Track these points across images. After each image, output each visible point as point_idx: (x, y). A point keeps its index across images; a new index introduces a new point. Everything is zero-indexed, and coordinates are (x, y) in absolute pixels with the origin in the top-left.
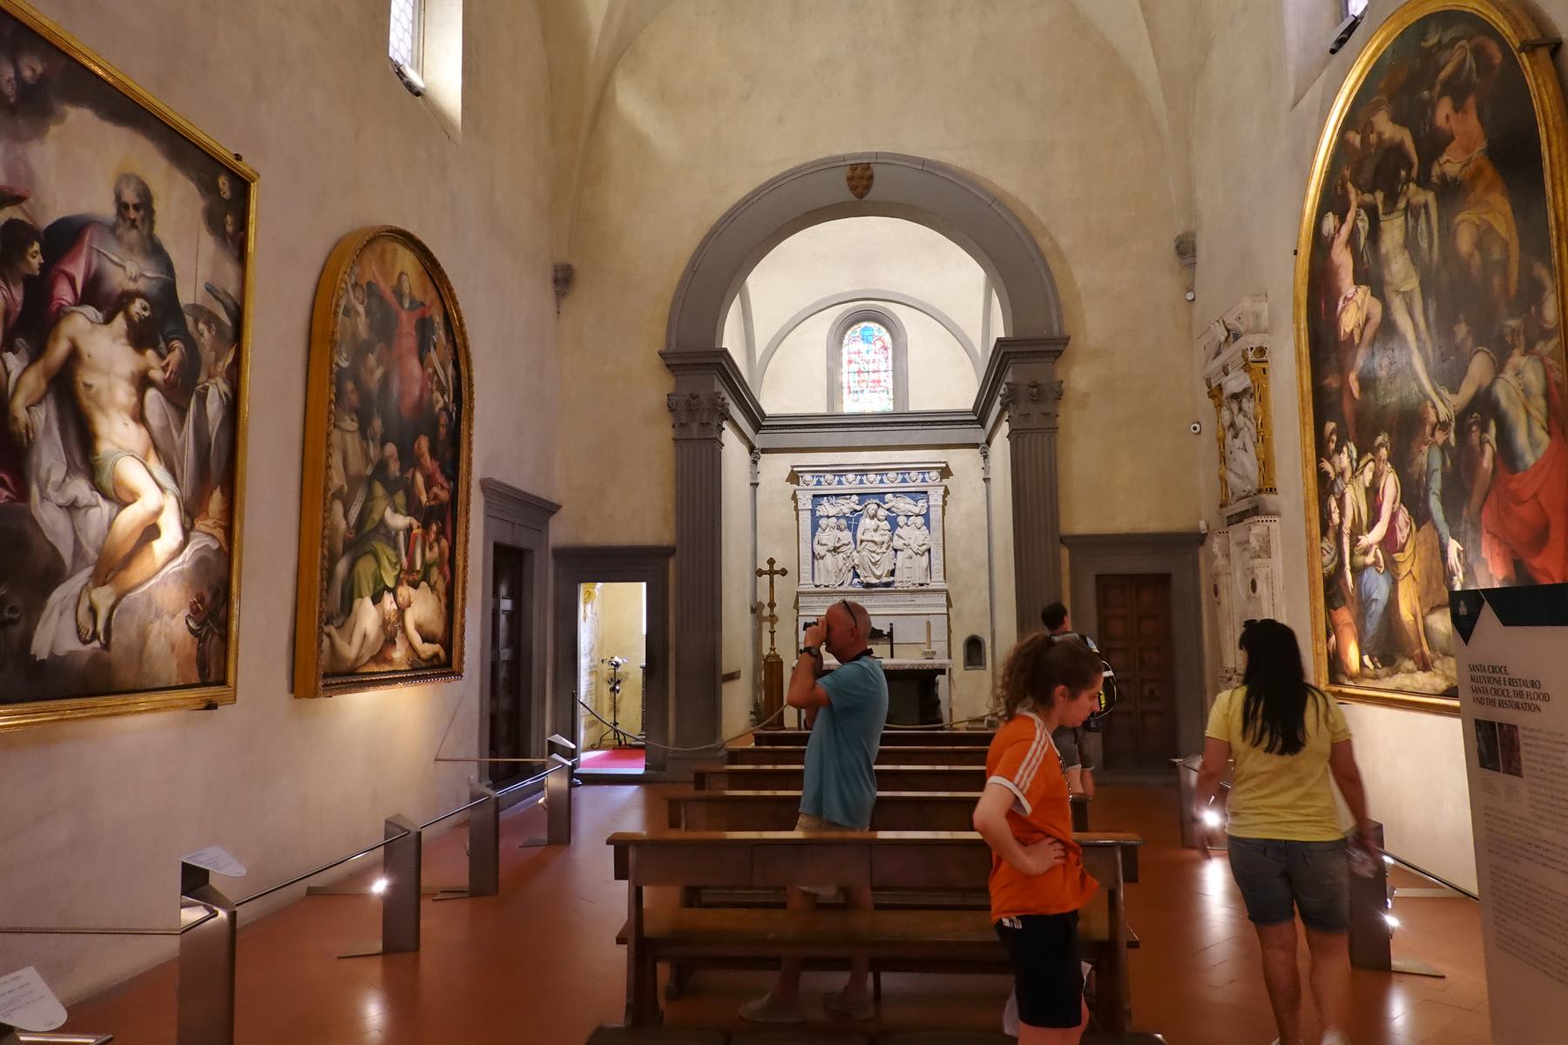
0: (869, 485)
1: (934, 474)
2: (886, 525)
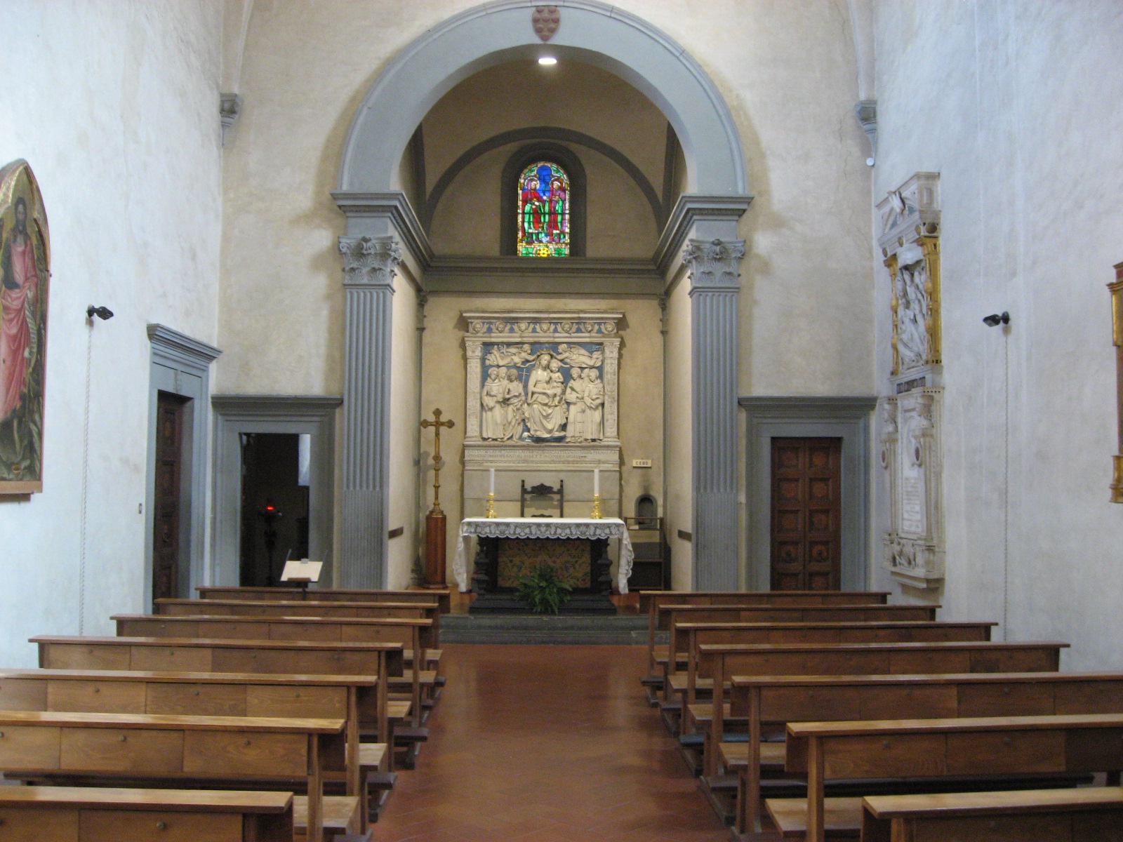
0: (542, 334)
1: (610, 327)
2: (558, 376)
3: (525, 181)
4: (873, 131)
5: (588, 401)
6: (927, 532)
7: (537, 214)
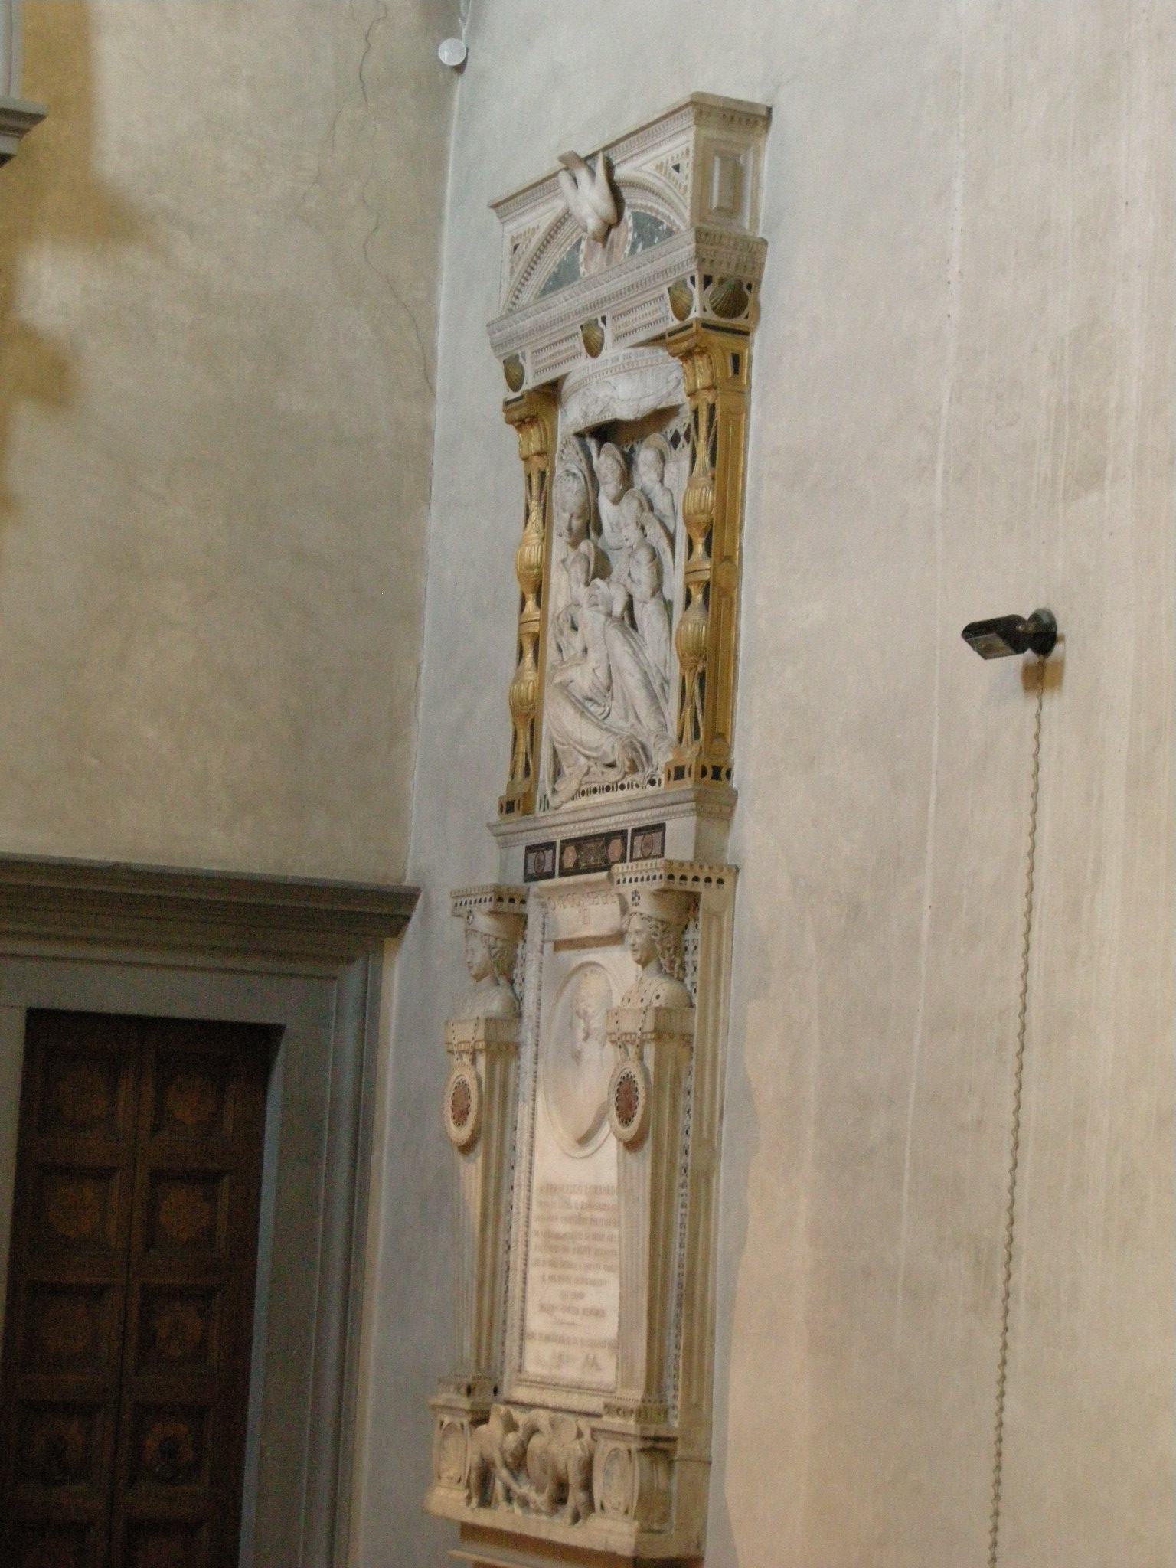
6: (648, 1390)
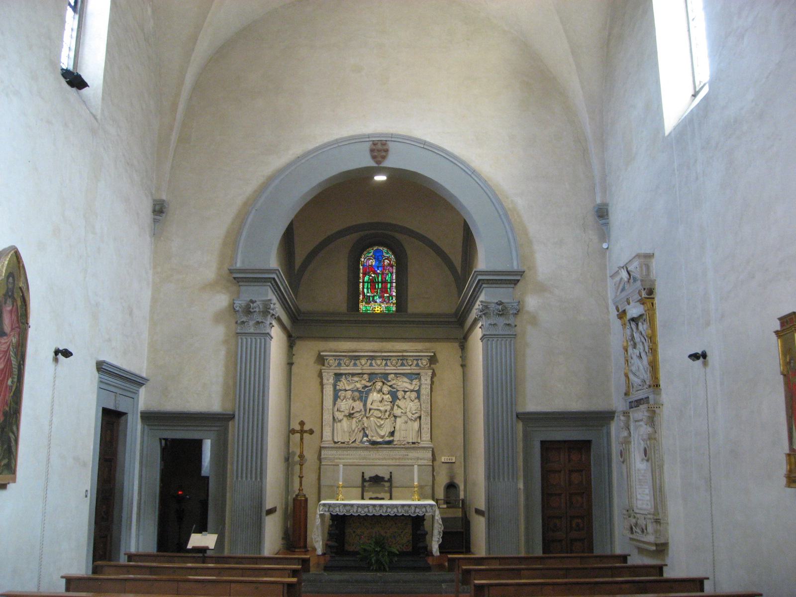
0: (377, 367)
1: (425, 362)
2: (388, 397)
3: (365, 259)
4: (607, 224)
5: (410, 415)
7: (373, 282)
